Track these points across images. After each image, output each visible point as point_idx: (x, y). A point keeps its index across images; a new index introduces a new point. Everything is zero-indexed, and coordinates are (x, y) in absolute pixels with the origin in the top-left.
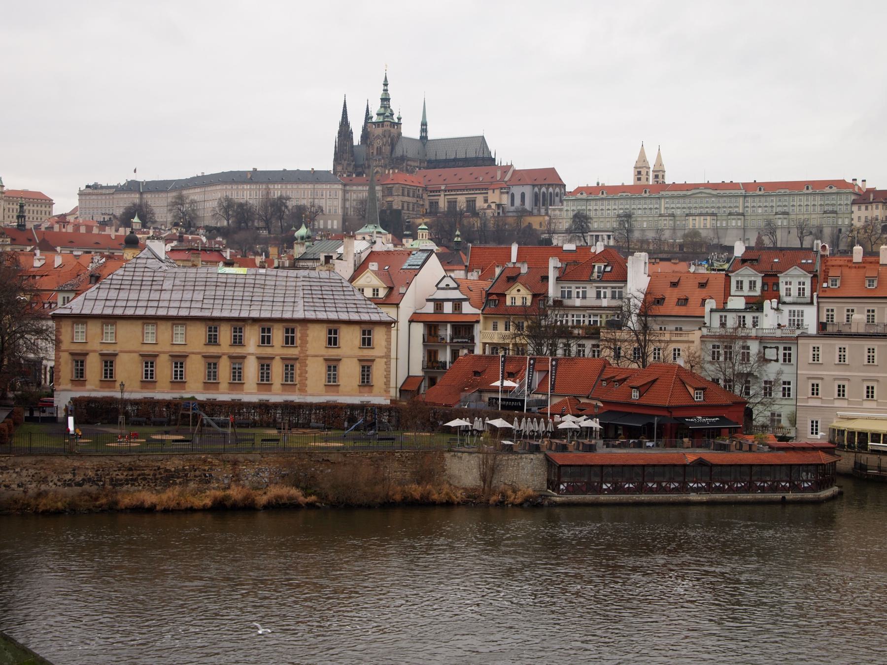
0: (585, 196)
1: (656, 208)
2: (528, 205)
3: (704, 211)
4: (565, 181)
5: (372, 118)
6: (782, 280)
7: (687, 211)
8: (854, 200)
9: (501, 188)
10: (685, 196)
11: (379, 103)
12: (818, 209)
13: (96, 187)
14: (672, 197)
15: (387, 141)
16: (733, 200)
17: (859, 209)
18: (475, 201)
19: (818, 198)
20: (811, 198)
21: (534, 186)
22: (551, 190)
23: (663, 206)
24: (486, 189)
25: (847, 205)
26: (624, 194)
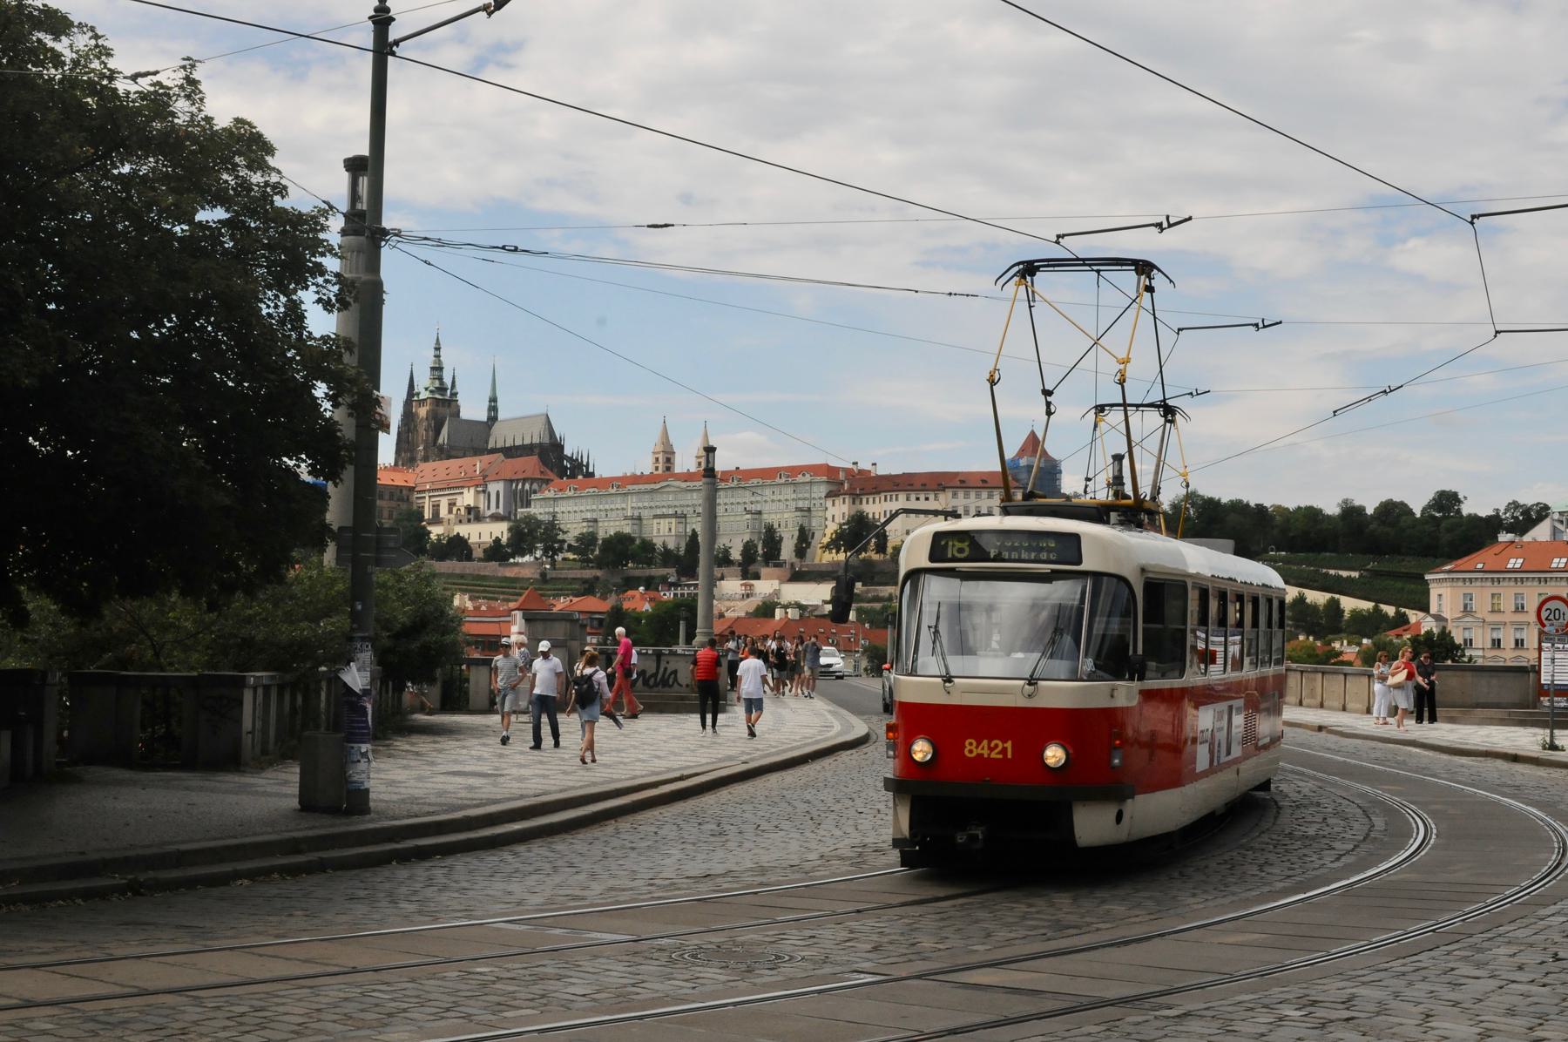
1: (623, 509)
2: (501, 511)
5: (418, 394)
8: (830, 491)
9: (477, 486)
10: (653, 491)
12: (793, 505)
15: (429, 425)
17: (833, 505)
18: (455, 504)
19: (790, 489)
20: (784, 489)
22: (527, 486)
24: (463, 487)
25: (820, 498)
26: (591, 490)
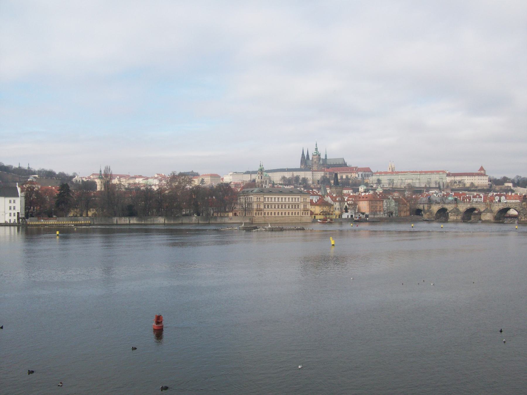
0: (379, 174)
3: (410, 178)
4: (372, 171)
6: (501, 197)
7: (405, 178)
9: (356, 173)
10: (405, 175)
11: (315, 150)
13: (236, 173)
14: (402, 175)
16: (417, 175)
17: (448, 178)
19: (438, 175)
20: (436, 175)
21: (364, 172)
22: (369, 173)
23: (400, 177)
26: (389, 174)
